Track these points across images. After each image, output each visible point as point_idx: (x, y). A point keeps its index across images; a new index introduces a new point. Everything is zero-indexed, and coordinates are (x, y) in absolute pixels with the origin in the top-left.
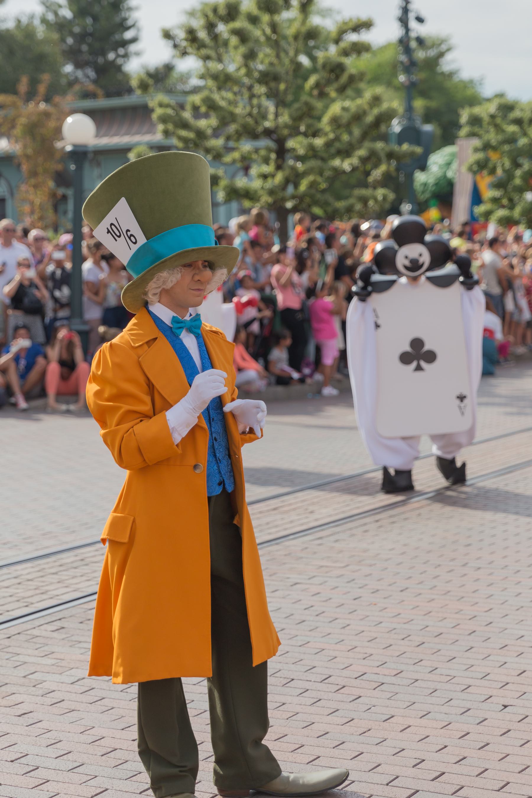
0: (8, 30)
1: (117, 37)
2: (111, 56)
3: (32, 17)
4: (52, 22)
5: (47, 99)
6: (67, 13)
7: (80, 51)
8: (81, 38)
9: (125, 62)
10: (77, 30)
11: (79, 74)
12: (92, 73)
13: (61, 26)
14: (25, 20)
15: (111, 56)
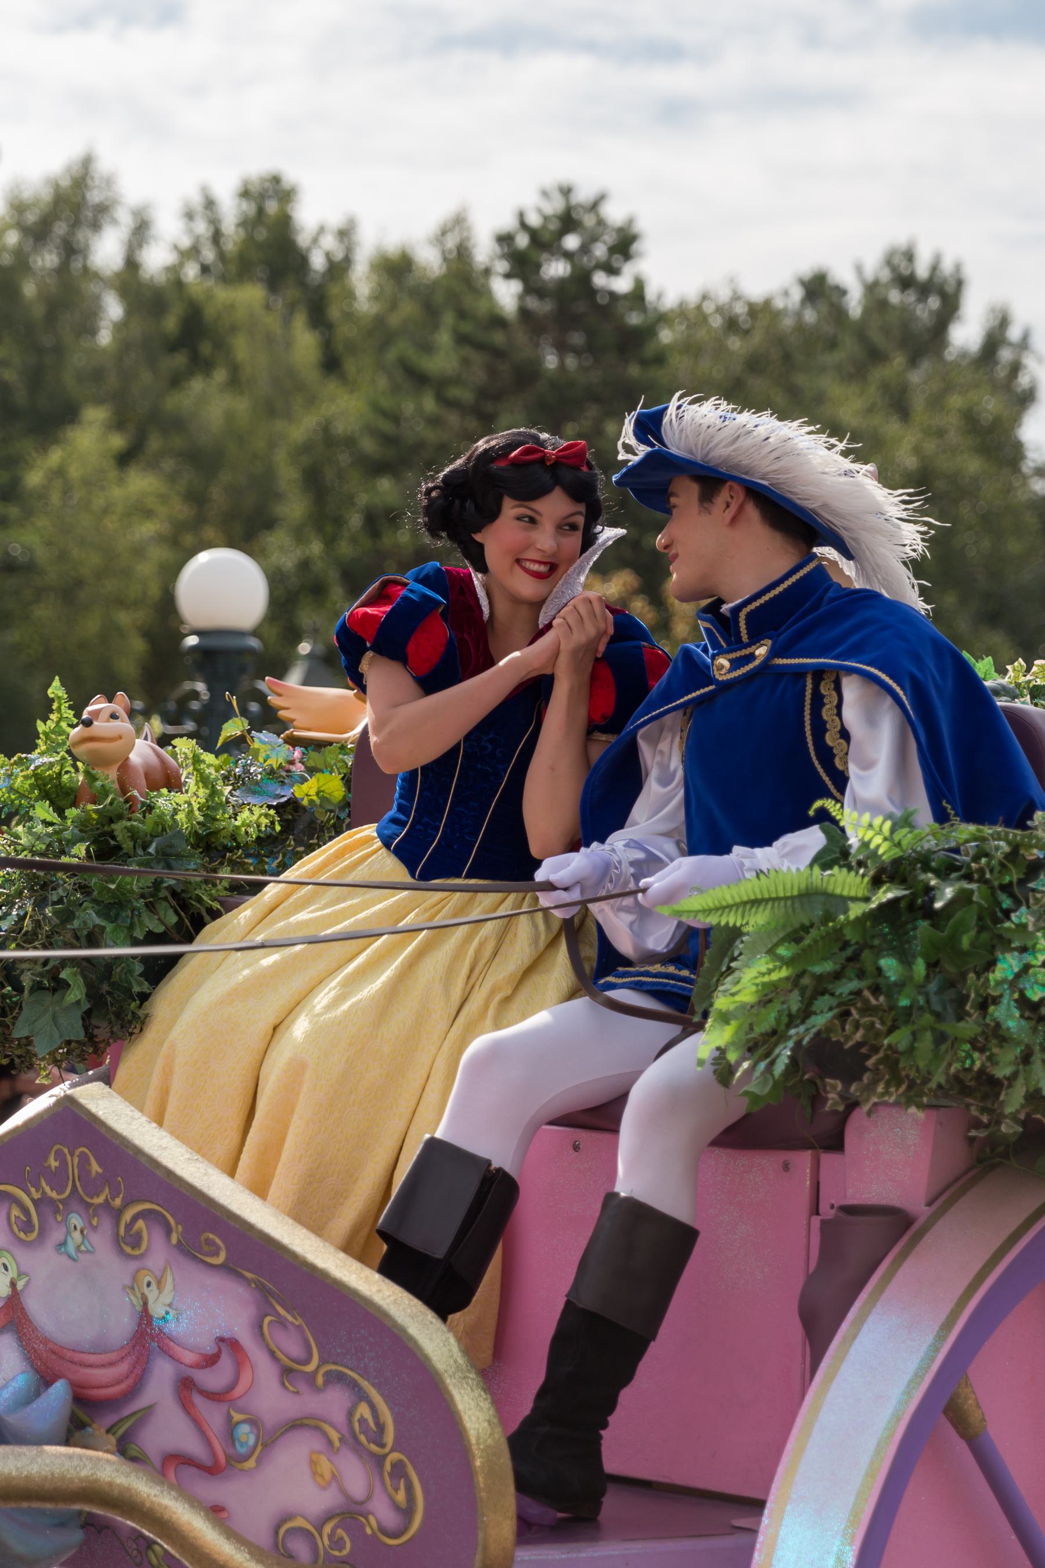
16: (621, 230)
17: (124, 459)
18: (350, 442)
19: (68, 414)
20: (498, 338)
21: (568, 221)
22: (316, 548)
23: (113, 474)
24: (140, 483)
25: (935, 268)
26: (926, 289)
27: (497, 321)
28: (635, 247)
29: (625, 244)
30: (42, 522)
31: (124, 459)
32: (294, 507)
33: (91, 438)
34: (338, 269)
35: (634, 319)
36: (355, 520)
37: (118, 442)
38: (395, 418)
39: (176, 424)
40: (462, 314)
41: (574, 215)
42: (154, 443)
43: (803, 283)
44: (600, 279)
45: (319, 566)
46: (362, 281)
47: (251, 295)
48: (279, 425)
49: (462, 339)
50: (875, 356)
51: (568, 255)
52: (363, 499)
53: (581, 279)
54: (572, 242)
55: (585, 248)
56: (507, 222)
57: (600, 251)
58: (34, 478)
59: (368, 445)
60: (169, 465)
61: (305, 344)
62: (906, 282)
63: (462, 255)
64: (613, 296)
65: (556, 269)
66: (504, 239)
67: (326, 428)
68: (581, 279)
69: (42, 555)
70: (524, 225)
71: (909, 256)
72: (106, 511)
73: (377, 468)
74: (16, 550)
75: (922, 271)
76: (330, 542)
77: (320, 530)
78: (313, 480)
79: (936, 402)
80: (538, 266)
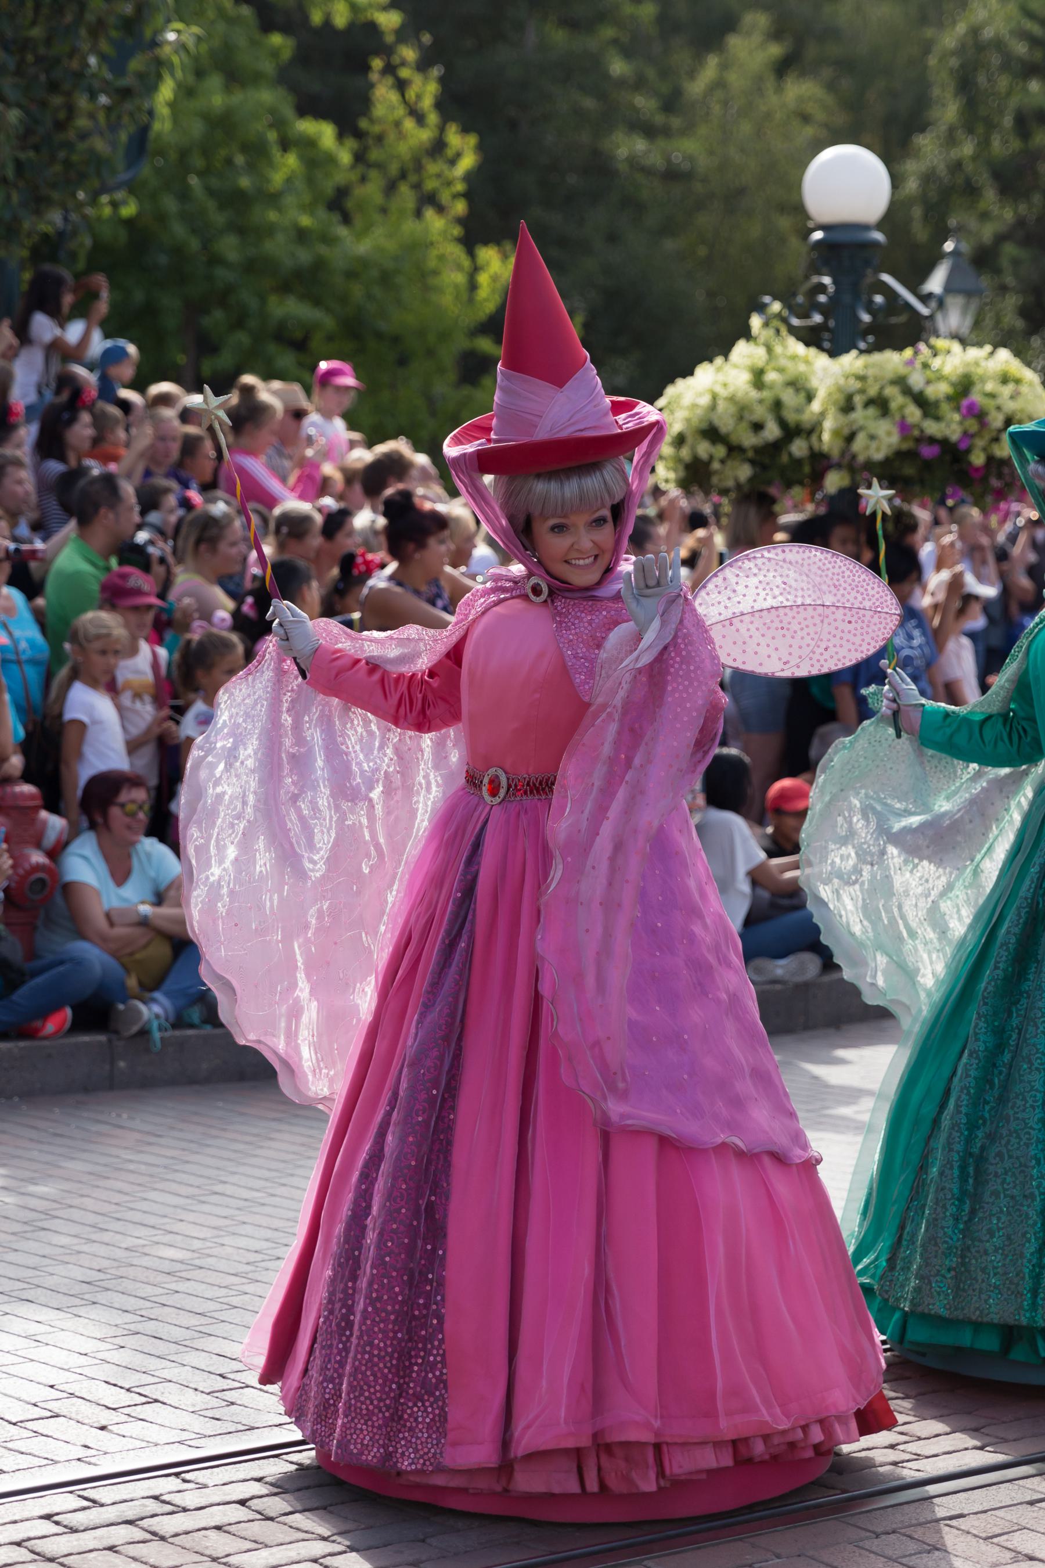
17: (783, 68)
18: (998, 44)
19: (729, 24)
22: (967, 149)
23: (770, 84)
24: (800, 90)
30: (703, 130)
31: (783, 68)
32: (949, 111)
33: (751, 48)
36: (1008, 121)
37: (775, 50)
39: (831, 33)
42: (812, 50)
45: (969, 167)
48: (929, 32)
52: (1014, 102)
58: (696, 87)
59: (1021, 49)
60: (827, 72)
67: (975, 31)
69: (704, 163)
72: (768, 116)
74: (677, 157)
76: (985, 143)
77: (970, 130)
78: (965, 83)
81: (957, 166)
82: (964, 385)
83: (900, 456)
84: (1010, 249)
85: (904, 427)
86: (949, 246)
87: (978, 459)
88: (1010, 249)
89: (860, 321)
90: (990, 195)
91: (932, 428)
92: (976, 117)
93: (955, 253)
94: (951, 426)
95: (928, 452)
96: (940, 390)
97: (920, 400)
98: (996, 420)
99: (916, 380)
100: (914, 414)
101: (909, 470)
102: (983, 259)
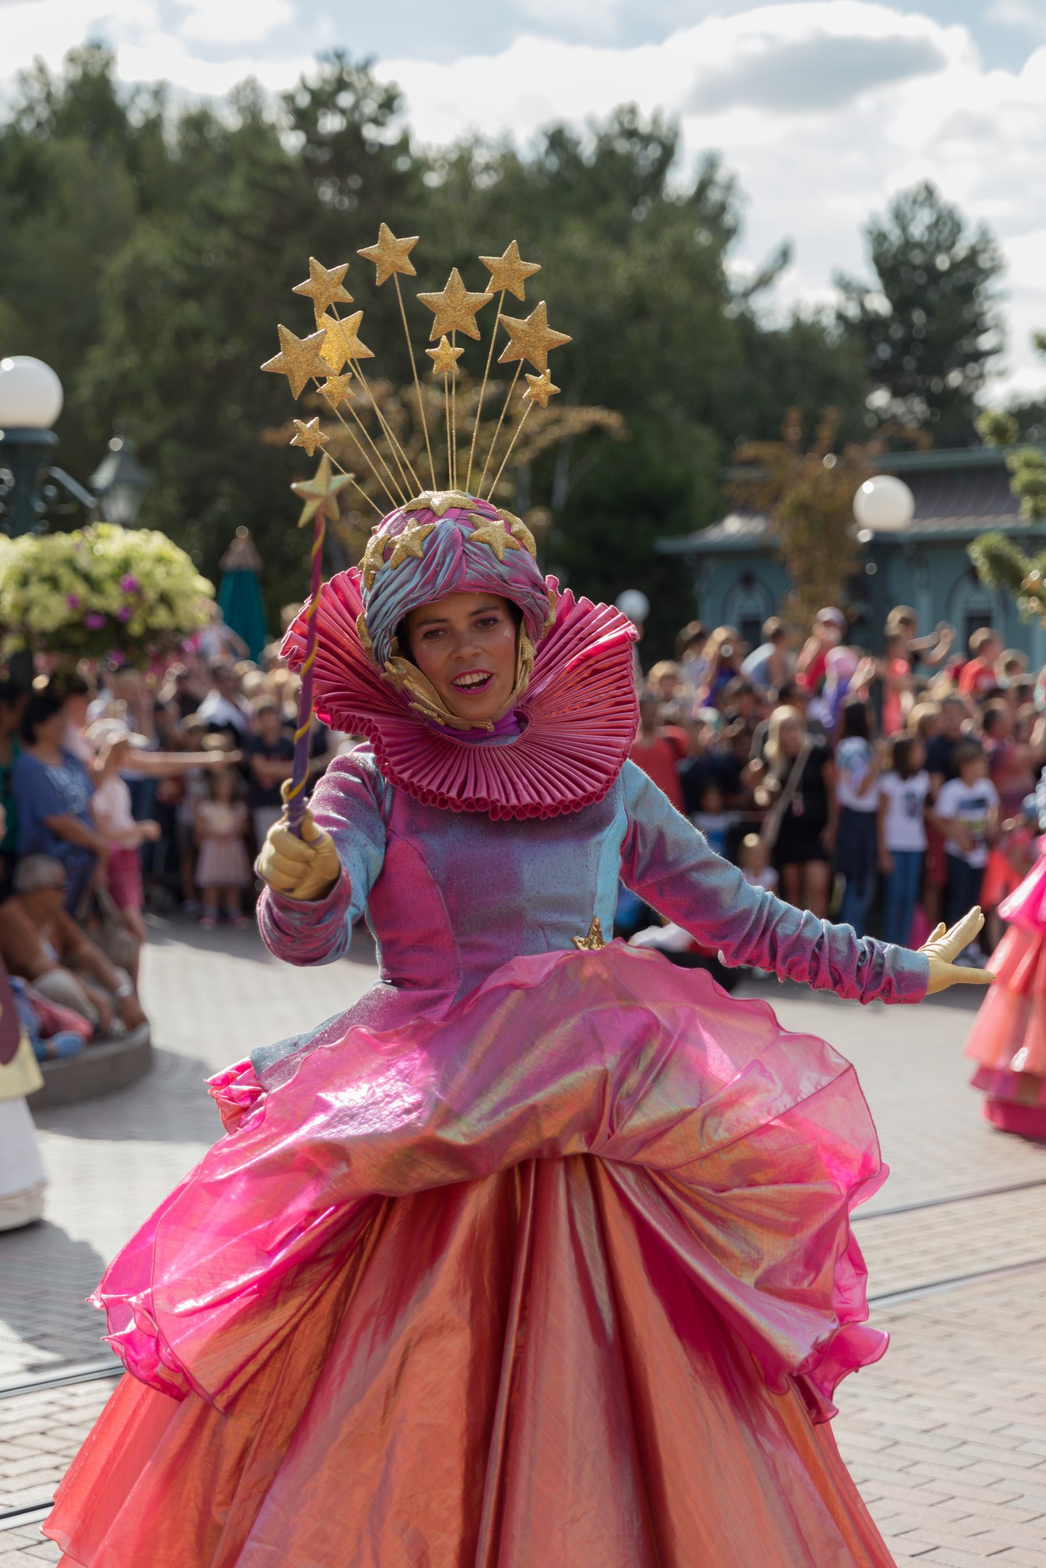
0: (775, 335)
1: (965, 345)
2: (955, 378)
3: (819, 311)
4: (856, 321)
5: (837, 449)
6: (880, 304)
7: (900, 368)
8: (903, 347)
9: (977, 388)
10: (897, 332)
11: (899, 408)
12: (919, 406)
13: (868, 327)
14: (807, 316)
15: (955, 378)
16: (386, 91)
20: (283, 182)
21: (341, 85)
25: (656, 121)
26: (647, 140)
27: (283, 167)
28: (396, 103)
29: (389, 103)
32: (116, 327)
34: (153, 126)
35: (403, 164)
36: (166, 336)
38: (199, 251)
40: (254, 162)
41: (346, 77)
43: (545, 134)
44: (370, 132)
46: (171, 136)
47: (76, 147)
49: (253, 184)
50: (604, 197)
51: (343, 112)
53: (353, 132)
54: (345, 100)
55: (356, 106)
56: (290, 84)
57: (370, 107)
59: (178, 276)
61: (122, 187)
62: (631, 134)
63: (252, 112)
64: (382, 147)
65: (331, 123)
66: (289, 99)
68: (353, 132)
70: (305, 87)
71: (633, 111)
73: (186, 293)
75: (644, 125)
78: (130, 305)
79: (652, 234)
80: (315, 121)
81: (123, 377)
82: (125, 565)
83: (71, 626)
84: (170, 449)
85: (73, 602)
86: (116, 444)
87: (136, 628)
88: (170, 449)
89: (31, 509)
90: (152, 402)
91: (97, 602)
92: (140, 334)
93: (121, 452)
94: (113, 601)
95: (94, 623)
96: (100, 570)
97: (87, 578)
98: (151, 595)
99: (83, 561)
100: (81, 589)
101: (77, 637)
102: (145, 456)
